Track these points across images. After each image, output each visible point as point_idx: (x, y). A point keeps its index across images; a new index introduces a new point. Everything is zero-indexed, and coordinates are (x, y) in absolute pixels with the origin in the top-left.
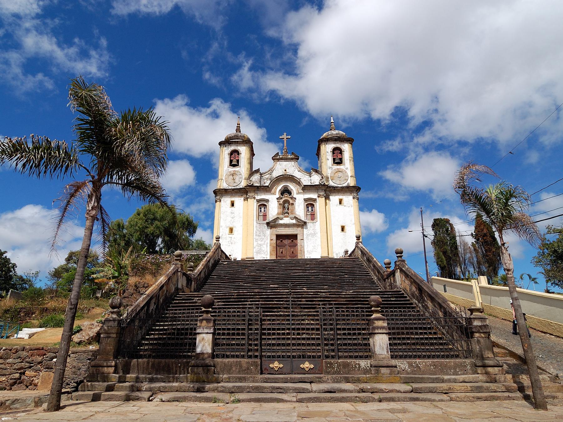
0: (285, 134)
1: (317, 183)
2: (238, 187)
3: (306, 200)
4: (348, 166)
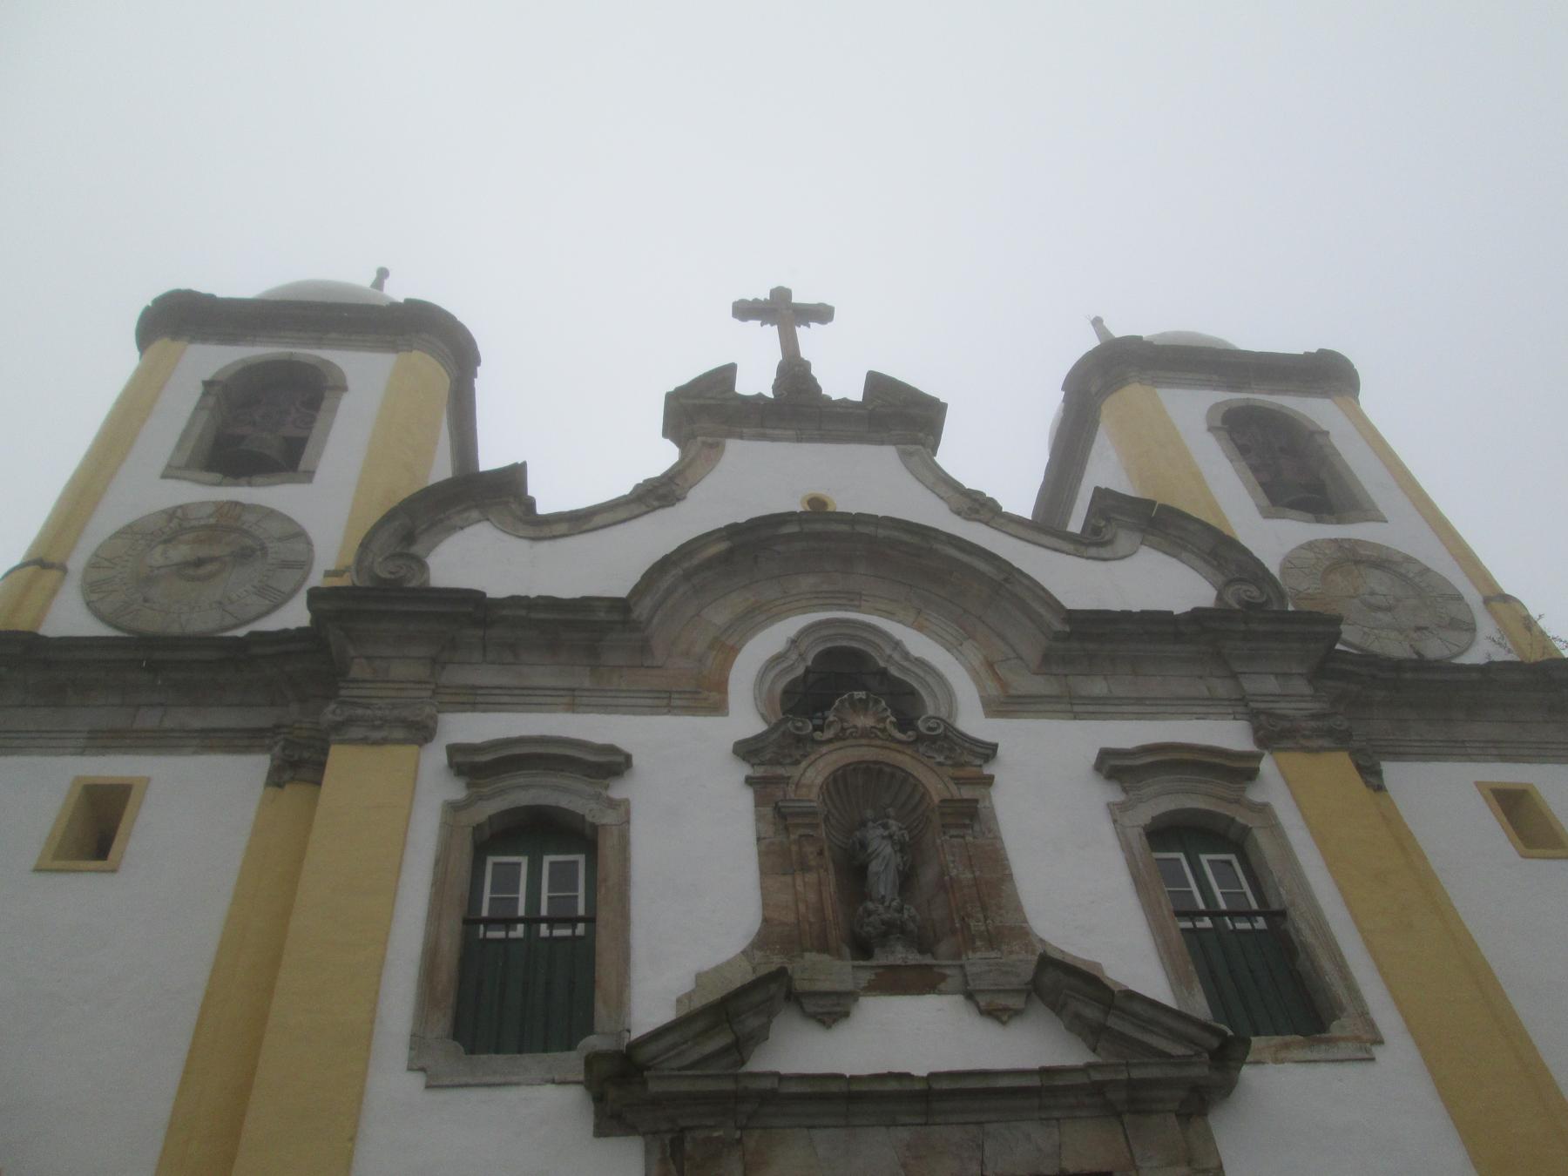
3: (1115, 767)
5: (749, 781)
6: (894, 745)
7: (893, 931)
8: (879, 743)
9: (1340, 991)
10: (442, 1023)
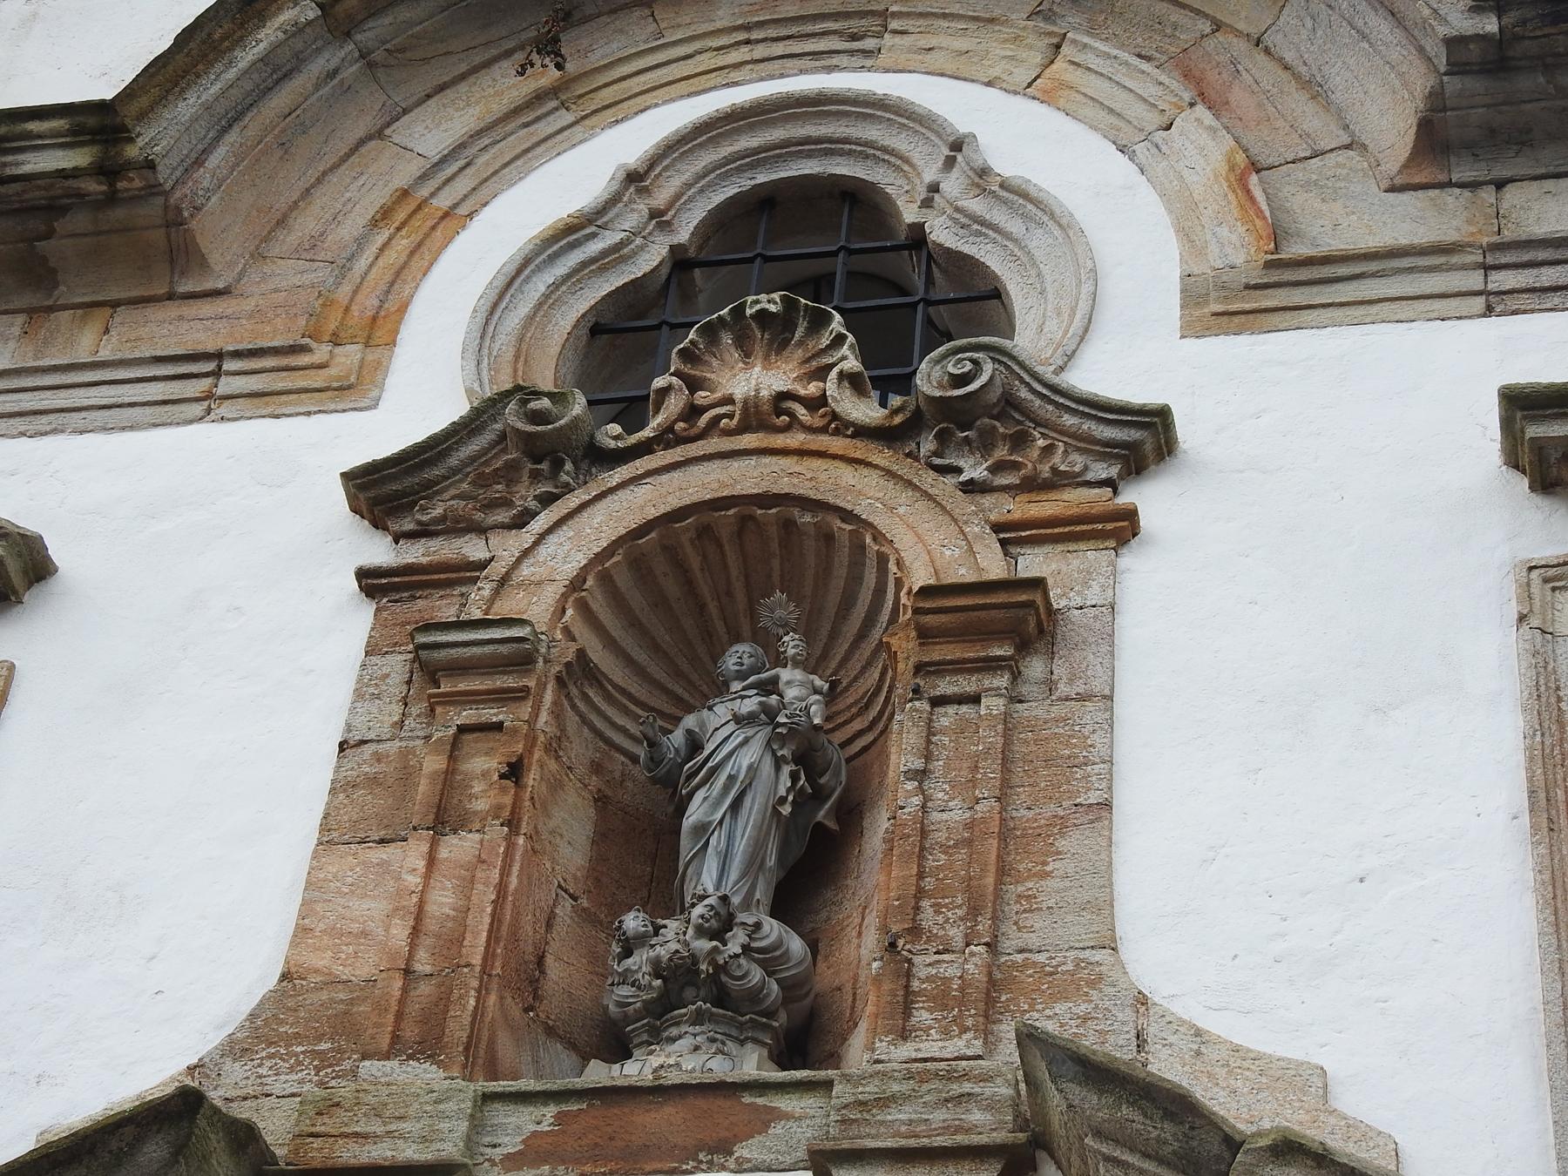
5: (372, 582)
6: (837, 444)
7: (687, 991)
8: (795, 439)
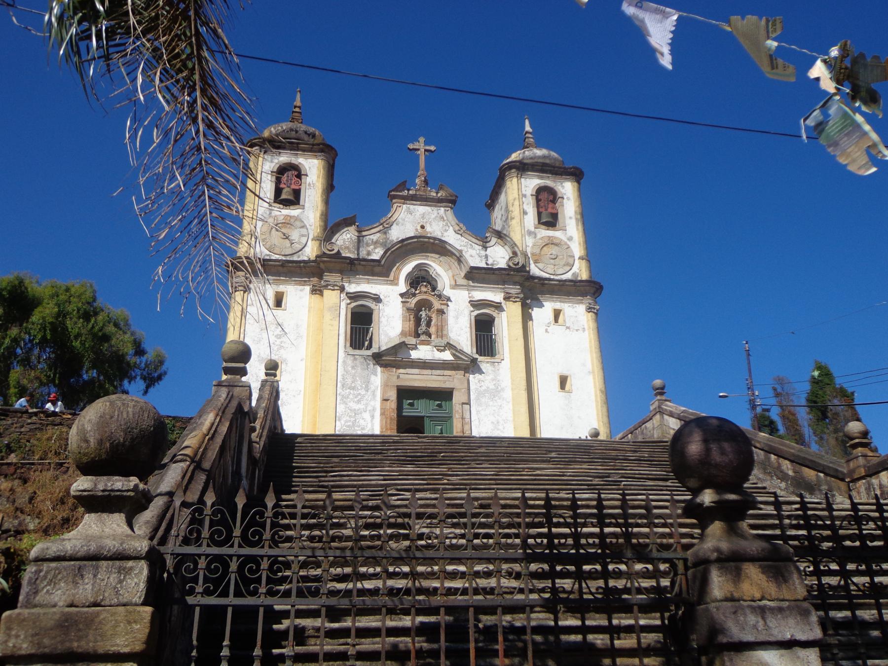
0: (422, 140)
1: (502, 264)
2: (295, 258)
4: (571, 231)
9: (500, 350)
10: (348, 344)
